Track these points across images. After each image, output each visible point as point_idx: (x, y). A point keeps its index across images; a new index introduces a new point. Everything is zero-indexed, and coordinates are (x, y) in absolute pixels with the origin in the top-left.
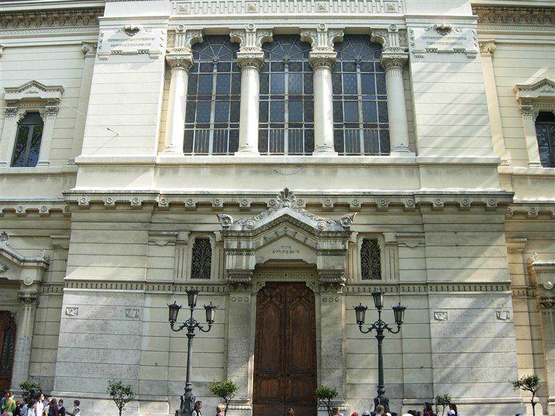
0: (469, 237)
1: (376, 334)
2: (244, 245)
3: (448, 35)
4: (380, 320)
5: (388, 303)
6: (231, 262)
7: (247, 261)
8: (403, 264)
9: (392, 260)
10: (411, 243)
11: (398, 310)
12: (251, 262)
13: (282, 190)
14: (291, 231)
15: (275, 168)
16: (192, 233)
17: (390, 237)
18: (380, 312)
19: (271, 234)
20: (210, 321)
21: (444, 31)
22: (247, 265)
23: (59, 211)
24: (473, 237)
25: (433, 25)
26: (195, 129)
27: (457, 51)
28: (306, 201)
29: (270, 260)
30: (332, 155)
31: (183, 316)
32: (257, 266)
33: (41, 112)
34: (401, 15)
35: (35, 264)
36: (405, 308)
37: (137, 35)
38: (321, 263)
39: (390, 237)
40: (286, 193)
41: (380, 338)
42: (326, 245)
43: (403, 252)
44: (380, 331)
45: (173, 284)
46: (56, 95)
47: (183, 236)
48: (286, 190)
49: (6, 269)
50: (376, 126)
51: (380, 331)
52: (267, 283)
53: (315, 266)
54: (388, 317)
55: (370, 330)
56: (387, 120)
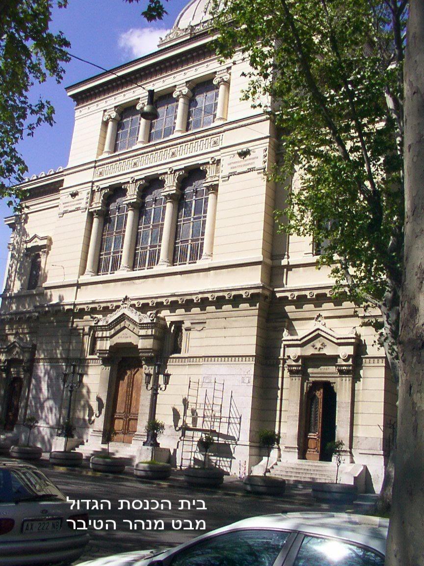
3: (248, 157)
8: (193, 343)
10: (199, 327)
13: (124, 297)
15: (134, 281)
19: (118, 327)
21: (244, 154)
25: (236, 152)
26: (104, 256)
27: (250, 170)
32: (111, 347)
34: (218, 148)
38: (141, 344)
39: (187, 324)
40: (126, 299)
42: (143, 332)
43: (193, 334)
46: (45, 242)
48: (126, 297)
50: (198, 240)
52: (123, 358)
53: (137, 346)
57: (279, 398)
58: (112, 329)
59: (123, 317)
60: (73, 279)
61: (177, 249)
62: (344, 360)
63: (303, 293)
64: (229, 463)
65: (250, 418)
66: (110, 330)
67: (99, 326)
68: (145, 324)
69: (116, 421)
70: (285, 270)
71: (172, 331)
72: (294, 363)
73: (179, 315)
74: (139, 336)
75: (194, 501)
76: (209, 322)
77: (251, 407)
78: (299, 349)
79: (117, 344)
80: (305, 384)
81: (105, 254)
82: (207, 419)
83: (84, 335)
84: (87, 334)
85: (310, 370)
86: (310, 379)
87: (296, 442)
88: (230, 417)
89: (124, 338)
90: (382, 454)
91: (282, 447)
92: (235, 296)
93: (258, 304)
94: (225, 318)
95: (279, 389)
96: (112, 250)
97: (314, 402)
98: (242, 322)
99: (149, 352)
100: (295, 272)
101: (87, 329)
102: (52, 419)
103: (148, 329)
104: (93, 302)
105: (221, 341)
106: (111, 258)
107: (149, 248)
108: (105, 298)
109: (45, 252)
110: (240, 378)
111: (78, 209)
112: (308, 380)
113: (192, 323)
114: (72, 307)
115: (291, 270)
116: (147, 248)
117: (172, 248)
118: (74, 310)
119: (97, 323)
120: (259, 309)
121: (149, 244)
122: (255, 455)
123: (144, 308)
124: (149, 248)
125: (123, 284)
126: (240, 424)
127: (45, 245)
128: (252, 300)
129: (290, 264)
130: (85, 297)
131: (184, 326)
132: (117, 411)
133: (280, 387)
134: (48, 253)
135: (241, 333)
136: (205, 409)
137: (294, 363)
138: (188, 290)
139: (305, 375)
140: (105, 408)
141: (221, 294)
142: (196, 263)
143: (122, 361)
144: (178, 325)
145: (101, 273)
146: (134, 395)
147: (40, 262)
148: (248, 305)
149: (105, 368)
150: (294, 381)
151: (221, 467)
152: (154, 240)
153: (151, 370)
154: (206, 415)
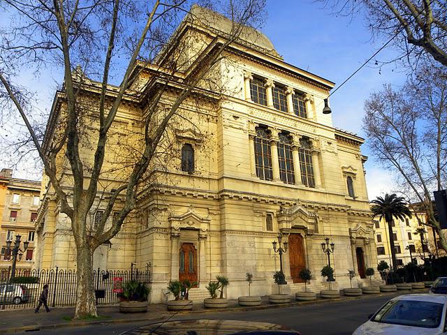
5: (330, 242)
6: (284, 225)
17: (321, 219)
20: (286, 248)
31: (278, 246)
33: (193, 145)
37: (238, 120)
41: (329, 254)
47: (264, 214)
49: (194, 223)
54: (330, 247)
111: (240, 129)
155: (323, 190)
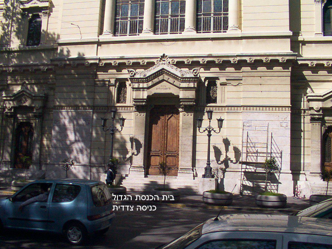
0: (268, 79)
1: (207, 133)
2: (141, 85)
4: (210, 126)
5: (216, 117)
7: (143, 94)
9: (223, 92)
11: (220, 121)
12: (144, 95)
13: (162, 55)
14: (166, 77)
16: (117, 80)
17: (223, 80)
18: (210, 122)
19: (156, 80)
22: (143, 96)
23: (51, 69)
24: (270, 80)
28: (176, 60)
29: (155, 94)
30: (194, 34)
32: (148, 96)
35: (40, 98)
36: (223, 120)
38: (182, 94)
39: (223, 80)
40: (164, 56)
41: (209, 135)
44: (209, 132)
45: (107, 106)
48: (164, 55)
51: (209, 132)
52: (155, 106)
53: (178, 96)
54: (214, 124)
55: (204, 131)
56: (227, 11)
57: (303, 138)
58: (149, 81)
59: (162, 72)
60: (94, 37)
61: (199, 20)
62: (316, 111)
63: (321, 62)
64: (276, 187)
65: (290, 153)
66: (148, 82)
67: (135, 79)
68: (188, 78)
69: (153, 158)
70: (301, 44)
71: (206, 85)
72: (316, 113)
73: (213, 73)
74: (180, 88)
75: (119, 206)
76: (245, 80)
77: (290, 144)
78: (321, 102)
79: (155, 94)
80: (323, 128)
81: (122, 19)
82: (278, 155)
83: (109, 86)
84: (113, 86)
85: (326, 118)
86: (326, 124)
87: (320, 169)
88: (271, 153)
89: (164, 88)
90: (291, 172)
91: (307, 173)
92: (119, 63)
93: (290, 68)
94: (261, 77)
95: (302, 131)
96: (129, 15)
97: (328, 140)
98: (276, 81)
99: (191, 101)
100: (308, 46)
101: (113, 81)
102: (83, 159)
103: (189, 82)
104: (210, 56)
105: (259, 94)
106: (129, 23)
107: (169, 17)
108: (154, 55)
109: (46, 13)
110: (278, 123)
112: (325, 125)
113: (226, 79)
114: (97, 62)
115: (305, 45)
116: (167, 17)
117: (113, 23)
118: (99, 64)
119: (133, 76)
120: (291, 72)
121: (170, 14)
122: (328, 182)
123: (180, 65)
124: (169, 17)
125: (151, 45)
126: (281, 157)
127: (47, 7)
128: (285, 65)
129: (305, 40)
130: (108, 53)
131: (218, 82)
132: (153, 149)
133: (303, 130)
134: (49, 15)
135: (277, 89)
136: (247, 147)
137: (316, 113)
138: (173, 54)
139: (323, 122)
140: (143, 147)
141: (258, 58)
142: (226, 32)
143: (157, 109)
144: (212, 81)
145: (119, 35)
146: (169, 136)
147: (41, 22)
148: (281, 68)
149: (139, 114)
150: (315, 125)
151: (272, 191)
152: (175, 11)
153: (190, 117)
154: (249, 151)
155: (238, 33)
